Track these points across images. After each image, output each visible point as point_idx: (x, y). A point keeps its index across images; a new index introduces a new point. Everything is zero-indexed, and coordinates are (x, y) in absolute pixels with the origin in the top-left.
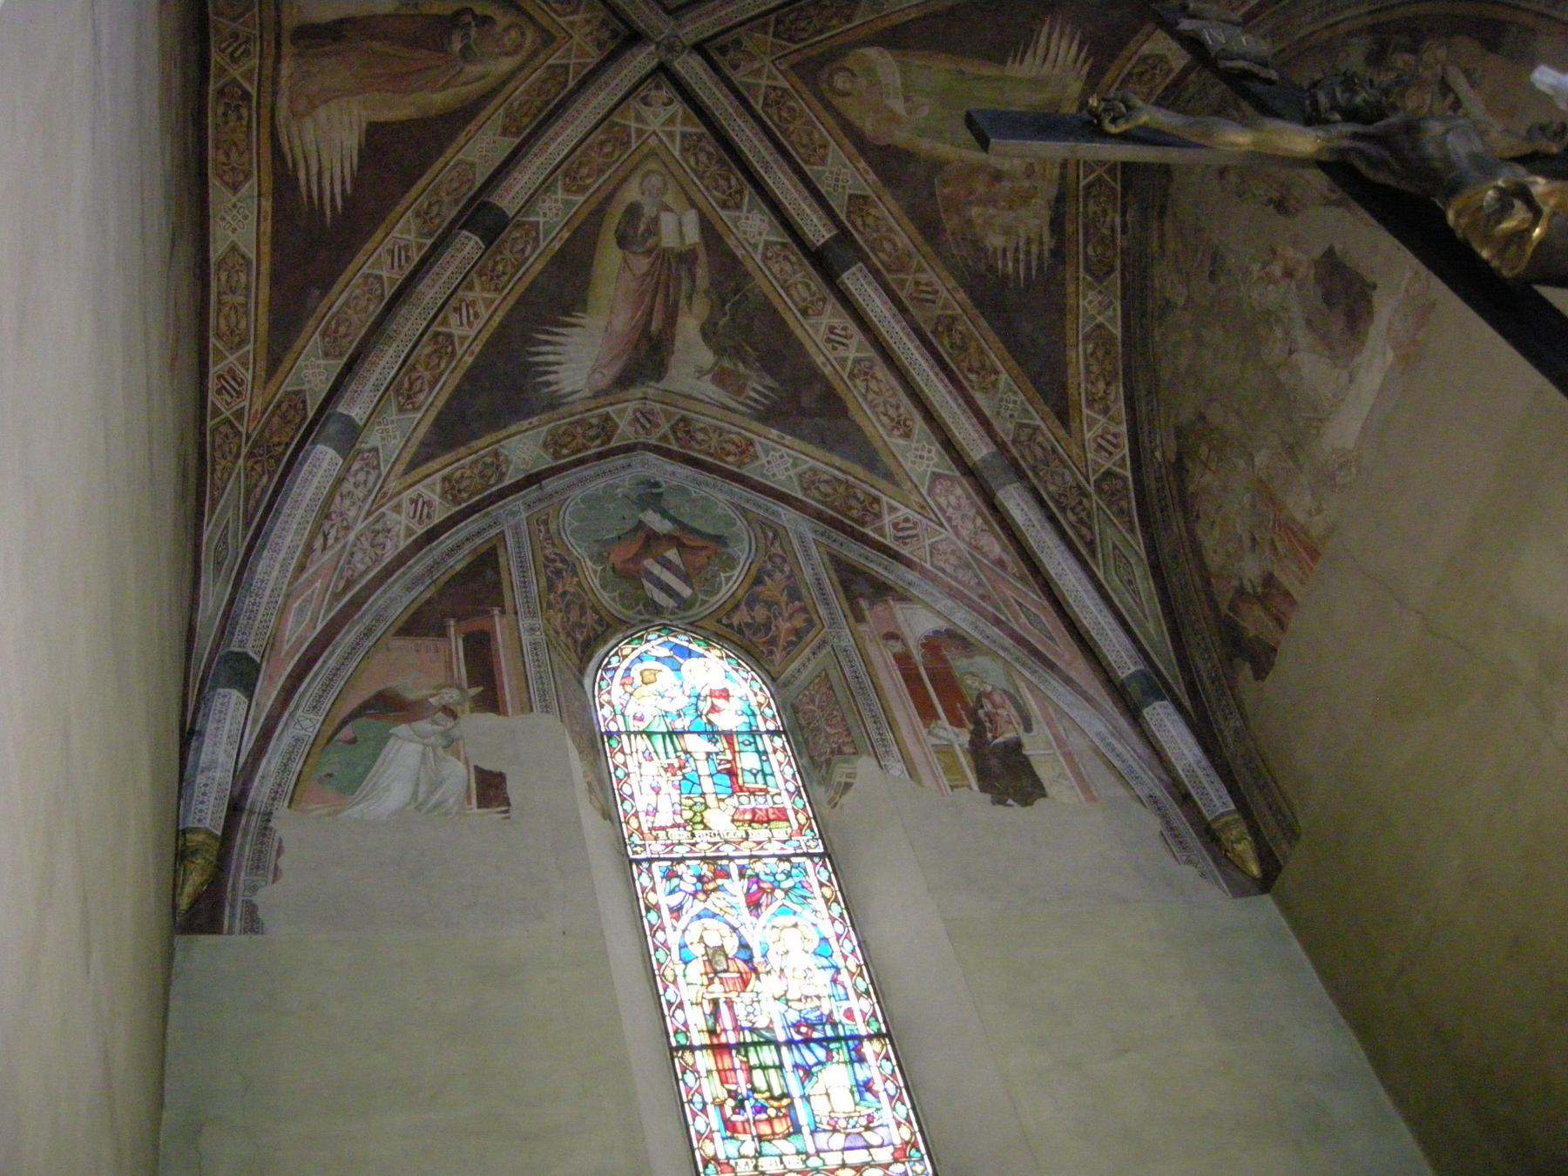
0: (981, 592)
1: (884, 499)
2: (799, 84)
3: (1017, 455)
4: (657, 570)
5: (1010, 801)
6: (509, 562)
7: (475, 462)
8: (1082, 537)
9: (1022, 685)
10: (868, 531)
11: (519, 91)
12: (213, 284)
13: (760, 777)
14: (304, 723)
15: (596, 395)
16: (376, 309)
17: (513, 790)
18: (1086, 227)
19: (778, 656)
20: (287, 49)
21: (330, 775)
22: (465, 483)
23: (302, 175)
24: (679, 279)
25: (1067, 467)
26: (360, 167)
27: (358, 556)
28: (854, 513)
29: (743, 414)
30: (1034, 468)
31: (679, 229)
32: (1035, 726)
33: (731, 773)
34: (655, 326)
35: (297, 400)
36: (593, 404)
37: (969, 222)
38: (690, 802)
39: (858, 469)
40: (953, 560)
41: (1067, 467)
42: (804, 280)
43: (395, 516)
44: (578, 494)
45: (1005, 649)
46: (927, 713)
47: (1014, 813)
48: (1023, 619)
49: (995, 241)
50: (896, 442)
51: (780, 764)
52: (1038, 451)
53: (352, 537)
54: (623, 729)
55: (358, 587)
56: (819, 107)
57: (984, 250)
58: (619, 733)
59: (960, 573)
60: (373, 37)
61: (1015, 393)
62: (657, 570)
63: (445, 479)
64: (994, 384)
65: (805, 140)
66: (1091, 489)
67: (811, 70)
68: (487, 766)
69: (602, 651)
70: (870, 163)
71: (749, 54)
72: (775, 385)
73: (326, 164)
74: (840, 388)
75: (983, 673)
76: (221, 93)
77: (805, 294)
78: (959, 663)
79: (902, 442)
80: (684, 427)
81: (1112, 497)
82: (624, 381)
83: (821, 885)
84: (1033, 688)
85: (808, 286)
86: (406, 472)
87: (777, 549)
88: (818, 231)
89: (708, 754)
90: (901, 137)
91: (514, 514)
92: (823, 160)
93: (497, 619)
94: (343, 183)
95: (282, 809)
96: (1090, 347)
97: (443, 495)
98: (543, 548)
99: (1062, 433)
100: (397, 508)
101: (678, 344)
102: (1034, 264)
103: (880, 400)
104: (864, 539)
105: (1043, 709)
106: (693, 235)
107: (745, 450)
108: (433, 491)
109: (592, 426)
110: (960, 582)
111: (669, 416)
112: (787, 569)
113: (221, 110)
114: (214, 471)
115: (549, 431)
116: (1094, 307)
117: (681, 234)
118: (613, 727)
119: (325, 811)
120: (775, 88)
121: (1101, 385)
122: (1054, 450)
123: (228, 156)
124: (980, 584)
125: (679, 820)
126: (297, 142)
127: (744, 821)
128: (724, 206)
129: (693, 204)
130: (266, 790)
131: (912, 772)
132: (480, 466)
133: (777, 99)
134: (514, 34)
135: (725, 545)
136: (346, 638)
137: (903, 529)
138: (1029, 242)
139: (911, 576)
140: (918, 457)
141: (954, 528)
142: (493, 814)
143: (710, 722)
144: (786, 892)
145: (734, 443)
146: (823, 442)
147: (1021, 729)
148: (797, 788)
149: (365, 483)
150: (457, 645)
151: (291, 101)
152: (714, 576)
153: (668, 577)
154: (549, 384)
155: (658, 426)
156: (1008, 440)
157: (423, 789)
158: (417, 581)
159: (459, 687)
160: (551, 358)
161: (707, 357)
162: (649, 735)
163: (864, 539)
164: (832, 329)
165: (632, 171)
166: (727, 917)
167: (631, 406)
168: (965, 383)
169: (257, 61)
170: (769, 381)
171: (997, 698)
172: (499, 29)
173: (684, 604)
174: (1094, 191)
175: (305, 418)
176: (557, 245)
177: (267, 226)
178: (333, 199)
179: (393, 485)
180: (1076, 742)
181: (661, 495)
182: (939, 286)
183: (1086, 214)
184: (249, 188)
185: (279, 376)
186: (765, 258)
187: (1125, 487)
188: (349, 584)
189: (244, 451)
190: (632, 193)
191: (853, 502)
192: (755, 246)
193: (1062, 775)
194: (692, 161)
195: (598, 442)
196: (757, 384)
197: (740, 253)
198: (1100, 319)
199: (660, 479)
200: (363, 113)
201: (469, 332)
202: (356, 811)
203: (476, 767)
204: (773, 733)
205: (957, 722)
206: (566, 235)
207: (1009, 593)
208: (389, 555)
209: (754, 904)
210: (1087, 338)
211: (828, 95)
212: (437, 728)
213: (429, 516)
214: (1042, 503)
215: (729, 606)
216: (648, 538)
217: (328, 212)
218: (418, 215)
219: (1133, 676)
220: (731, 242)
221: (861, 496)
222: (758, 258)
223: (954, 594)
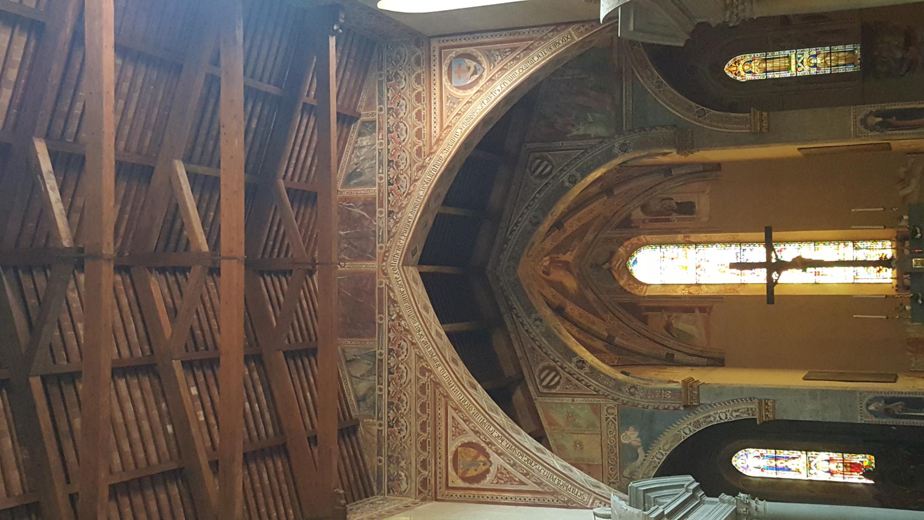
14: (672, 343)
46: (669, 220)
205: (670, 215)
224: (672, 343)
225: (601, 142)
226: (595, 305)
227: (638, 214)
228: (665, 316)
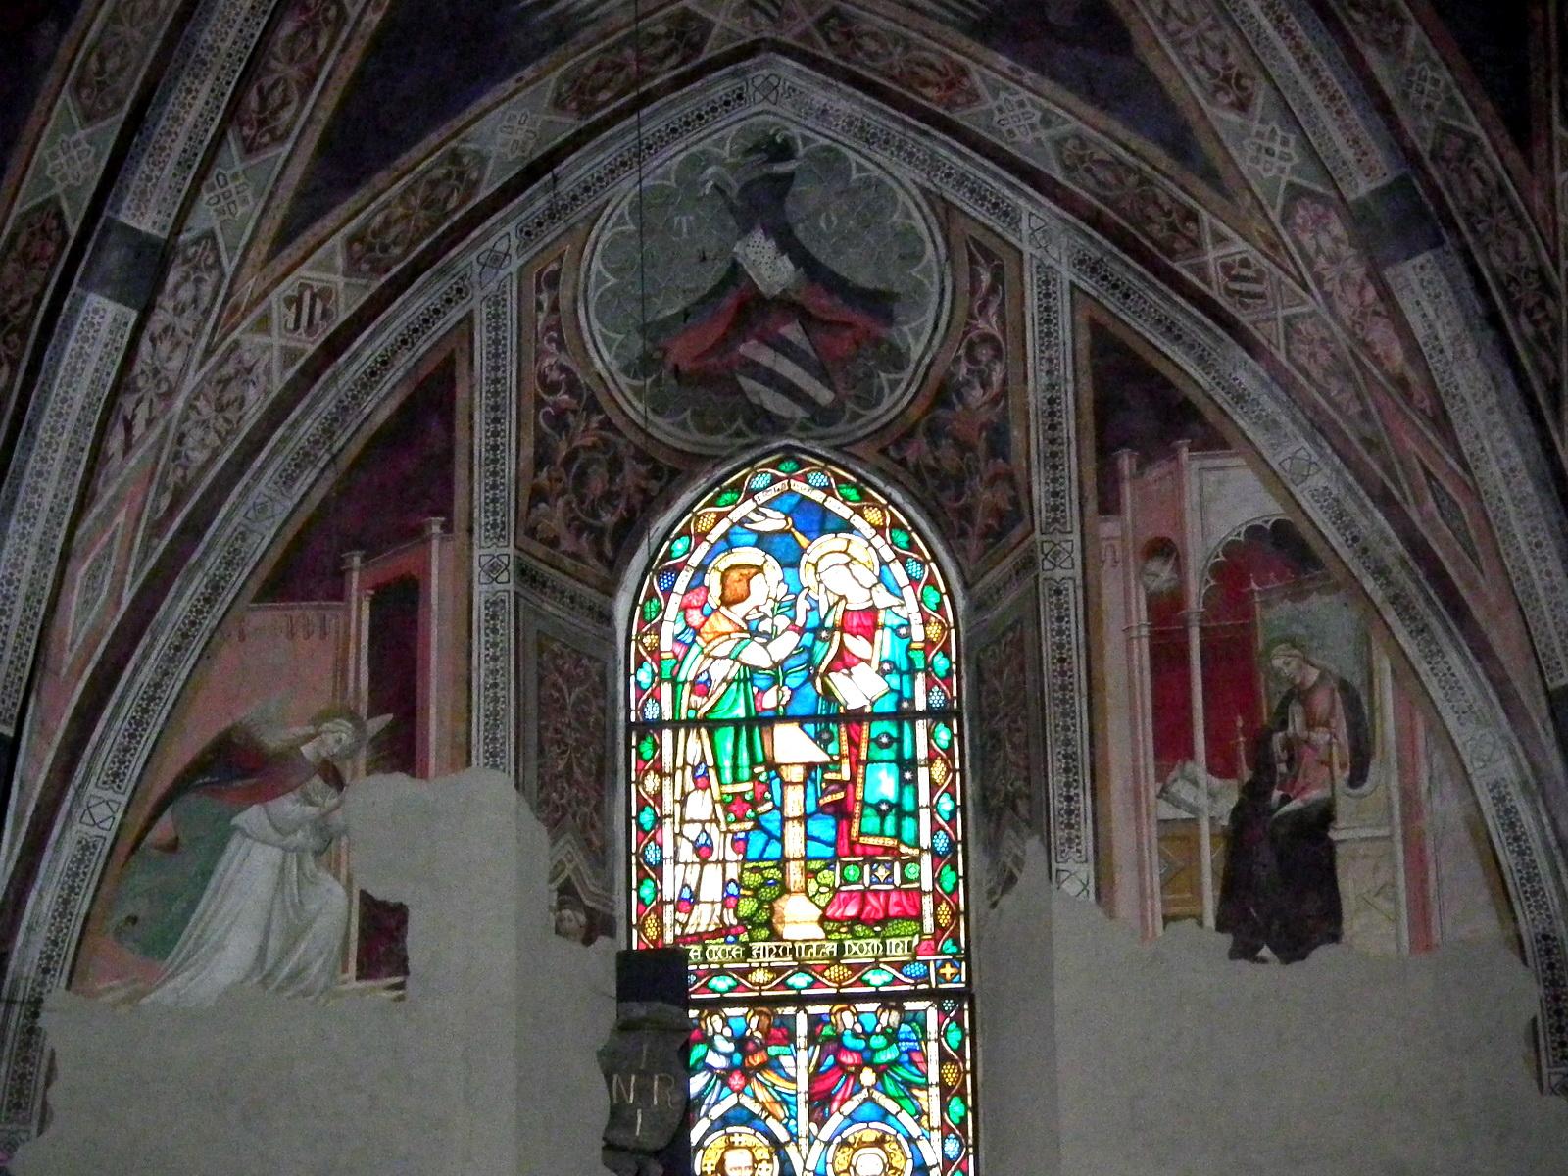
0: (1367, 430)
1: (1205, 215)
3: (1440, 182)
4: (766, 357)
5: (1265, 952)
6: (474, 398)
7: (410, 190)
8: (1542, 371)
9: (1384, 665)
13: (890, 820)
17: (417, 942)
21: (134, 920)
25: (1522, 226)
29: (942, 20)
30: (1468, 215)
32: (1374, 771)
33: (841, 812)
38: (756, 879)
39: (1155, 152)
40: (1323, 356)
41: (1522, 226)
43: (260, 339)
45: (1380, 572)
46: (1171, 744)
47: (1268, 973)
50: (1223, 116)
51: (934, 786)
52: (1477, 187)
53: (179, 404)
54: (668, 716)
55: (196, 496)
58: (659, 725)
59: (1334, 386)
61: (1434, 66)
62: (766, 357)
63: (351, 240)
64: (1399, 38)
68: (379, 893)
69: (661, 524)
75: (1307, 639)
78: (1273, 612)
79: (1233, 117)
83: (944, 1058)
84: (1405, 671)
86: (272, 255)
87: (989, 325)
89: (810, 767)
93: (435, 543)
95: (57, 995)
97: (352, 267)
98: (540, 354)
99: (1513, 156)
100: (263, 325)
105: (1406, 734)
107: (954, 79)
108: (330, 268)
109: (654, 39)
110: (1330, 400)
118: (651, 713)
119: (123, 992)
122: (1502, 190)
124: (1365, 414)
125: (730, 919)
127: (840, 921)
130: (30, 971)
131: (1103, 889)
132: (422, 190)
135: (889, 319)
136: (177, 608)
137: (1245, 279)
139: (1246, 374)
141: (1327, 296)
142: (379, 991)
143: (828, 694)
144: (881, 1071)
145: (932, 66)
146: (1092, 91)
147: (1342, 776)
148: (952, 845)
149: (195, 300)
150: (360, 613)
153: (788, 369)
155: (791, 16)
156: (1424, 148)
157: (274, 944)
159: (353, 716)
162: (710, 725)
166: (772, 1123)
168: (1349, 27)
171: (1321, 702)
173: (822, 416)
175: (65, 236)
179: (249, 286)
180: (1444, 808)
181: (790, 177)
191: (1151, 210)
193: (1386, 889)
195: (674, 60)
202: (163, 995)
203: (364, 894)
204: (935, 715)
205: (1222, 765)
207: (1411, 445)
208: (253, 413)
209: (820, 1101)
212: (310, 810)
213: (325, 314)
215: (896, 431)
216: (742, 307)
221: (1163, 199)
223: (1320, 428)
224: (98, 811)
226: (424, 157)
227: (1222, 502)
228: (338, 736)
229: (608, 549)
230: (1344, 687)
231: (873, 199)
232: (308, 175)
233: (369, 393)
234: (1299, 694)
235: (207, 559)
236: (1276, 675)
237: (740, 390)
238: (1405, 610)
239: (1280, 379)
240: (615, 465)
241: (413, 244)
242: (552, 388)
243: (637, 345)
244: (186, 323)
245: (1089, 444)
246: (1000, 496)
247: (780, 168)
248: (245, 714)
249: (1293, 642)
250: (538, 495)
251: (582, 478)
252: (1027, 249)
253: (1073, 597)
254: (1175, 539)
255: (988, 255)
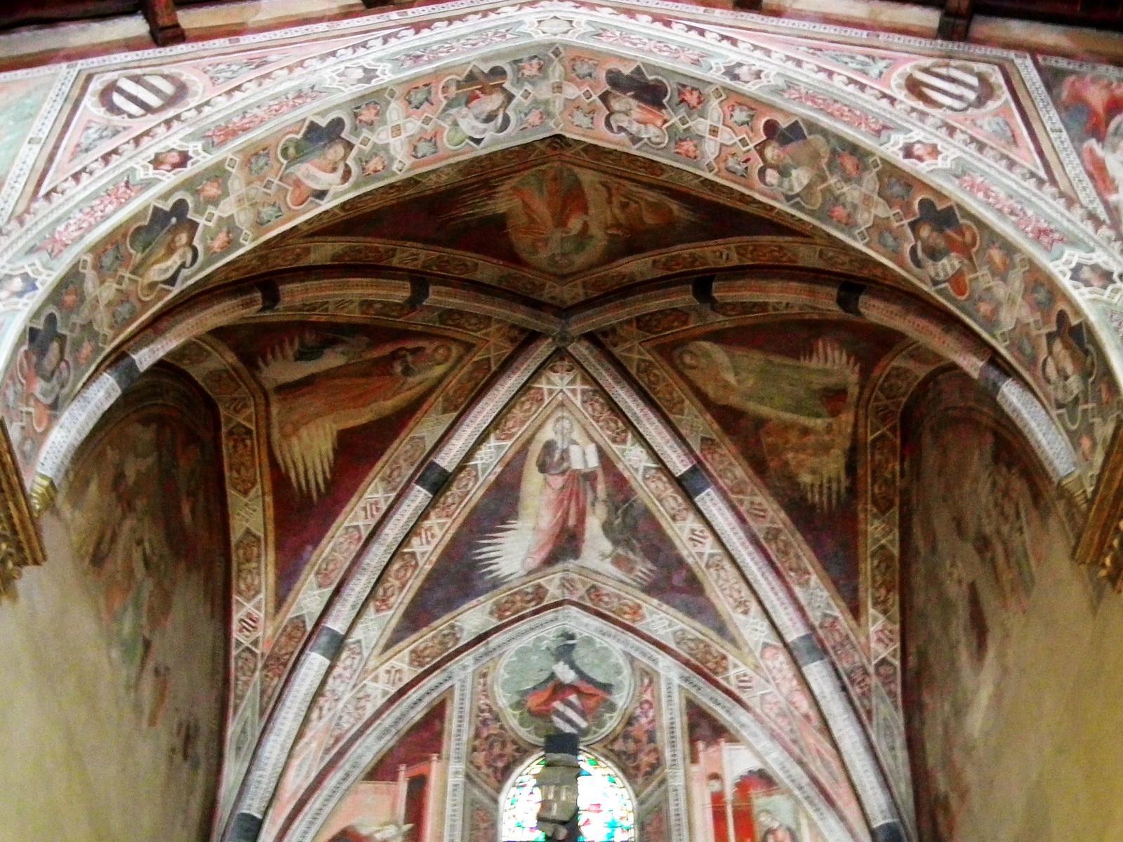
2: (659, 358)
6: (452, 712)
7: (434, 637)
8: (864, 707)
9: (804, 822)
10: (719, 679)
11: (452, 383)
12: (234, 558)
15: (530, 573)
16: (355, 548)
18: (874, 472)
19: (640, 780)
20: (273, 398)
22: (427, 652)
23: (293, 475)
24: (585, 490)
26: (335, 460)
27: (346, 717)
28: (710, 665)
30: (834, 648)
31: (584, 457)
34: (571, 522)
35: (299, 622)
36: (528, 579)
37: (786, 463)
39: (712, 634)
42: (673, 499)
43: (374, 684)
44: (515, 646)
45: (801, 788)
48: (819, 763)
49: (806, 478)
50: (738, 617)
56: (676, 376)
57: (798, 484)
59: (780, 720)
60: (334, 378)
63: (413, 652)
64: (807, 581)
65: (668, 397)
66: (871, 670)
67: (669, 351)
70: (713, 416)
71: (622, 337)
72: (654, 568)
73: (309, 465)
74: (700, 575)
76: (230, 433)
77: (673, 504)
78: (760, 801)
79: (742, 617)
80: (594, 591)
81: (887, 680)
82: (551, 560)
84: (812, 825)
85: (675, 499)
87: (647, 696)
88: (680, 465)
90: (734, 400)
91: (464, 668)
92: (681, 412)
94: (324, 473)
96: (876, 562)
97: (411, 663)
99: (853, 623)
100: (376, 679)
101: (587, 535)
102: (834, 496)
103: (726, 586)
104: (717, 685)
106: (593, 462)
107: (636, 610)
108: (403, 662)
109: (527, 594)
111: (584, 583)
112: (651, 714)
113: (231, 444)
114: (236, 685)
115: (495, 603)
116: (877, 532)
117: (585, 461)
120: (644, 361)
121: (883, 591)
122: (847, 637)
123: (238, 472)
124: (792, 731)
126: (288, 455)
128: (614, 441)
129: (593, 440)
132: (440, 637)
133: (646, 368)
134: (441, 351)
135: (610, 693)
136: (331, 781)
138: (830, 481)
139: (744, 717)
140: (752, 629)
141: (777, 685)
150: (402, 787)
151: (281, 429)
152: (602, 716)
153: (571, 713)
154: (491, 572)
156: (817, 624)
158: (387, 731)
159: (396, 823)
160: (492, 555)
161: (607, 546)
163: (717, 685)
164: (693, 531)
165: (548, 417)
167: (559, 575)
169: (252, 409)
170: (650, 565)
172: (429, 351)
174: (879, 444)
176: (492, 478)
177: (270, 513)
178: (317, 484)
179: (372, 663)
181: (573, 646)
182: (766, 505)
183: (873, 460)
184: (256, 491)
185: (284, 609)
186: (645, 479)
187: (895, 673)
188: (337, 740)
189: (260, 665)
190: (548, 434)
191: (709, 657)
192: (637, 470)
194: (590, 409)
196: (643, 567)
197: (626, 474)
198: (883, 541)
199: (576, 631)
200: (334, 426)
201: (427, 549)
206: (499, 470)
208: (370, 711)
210: (873, 555)
211: (681, 367)
214: (839, 677)
215: (611, 737)
217: (314, 494)
218: (383, 479)
219: (881, 827)
220: (620, 467)
222: (639, 478)
223: (774, 736)
225: (1092, 217)
227: (736, 761)
229: (499, 775)
230: (789, 829)
231: (604, 654)
232: (400, 623)
233: (413, 710)
234: (770, 831)
235: (345, 764)
236: (760, 823)
237: (551, 721)
238: (811, 803)
239: (757, 718)
240: (504, 744)
241: (434, 658)
242: (482, 711)
243: (516, 698)
244: (347, 674)
245: (687, 738)
246: (651, 759)
247: (571, 642)
248: (353, 821)
249: (768, 812)
250: (474, 749)
251: (491, 746)
252: (662, 672)
253: (682, 793)
254: (719, 772)
255: (647, 673)
